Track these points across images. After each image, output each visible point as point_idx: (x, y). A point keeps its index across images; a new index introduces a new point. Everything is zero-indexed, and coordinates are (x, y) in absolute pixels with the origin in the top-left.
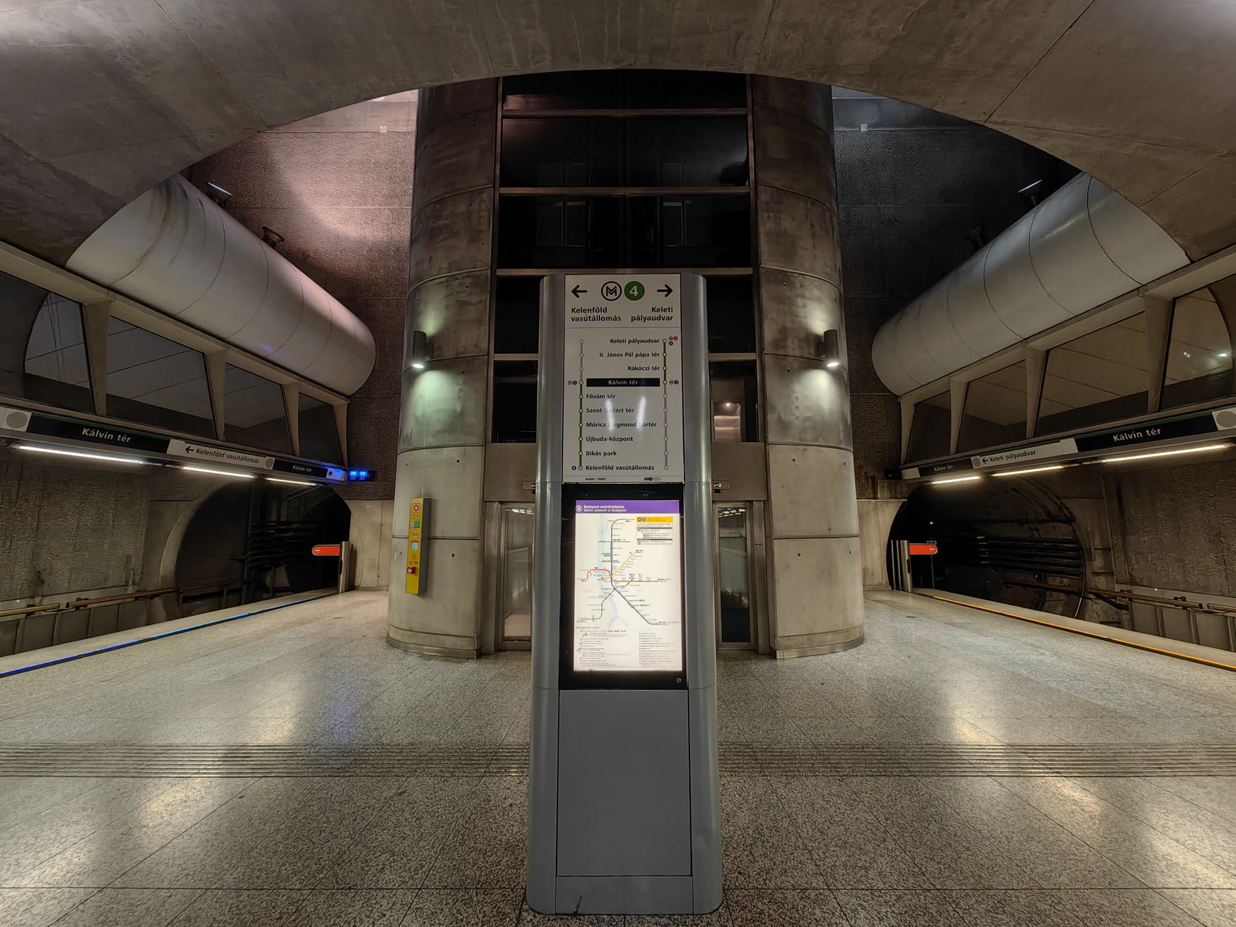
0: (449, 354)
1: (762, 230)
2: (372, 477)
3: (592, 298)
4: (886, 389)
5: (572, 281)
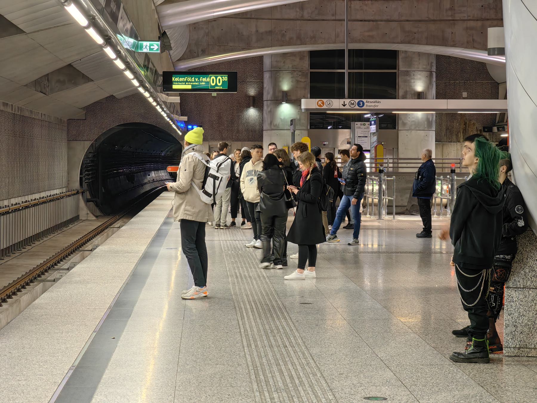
0: (293, 98)
1: (400, 57)
3: (359, 125)
4: (492, 79)
5: (356, 123)
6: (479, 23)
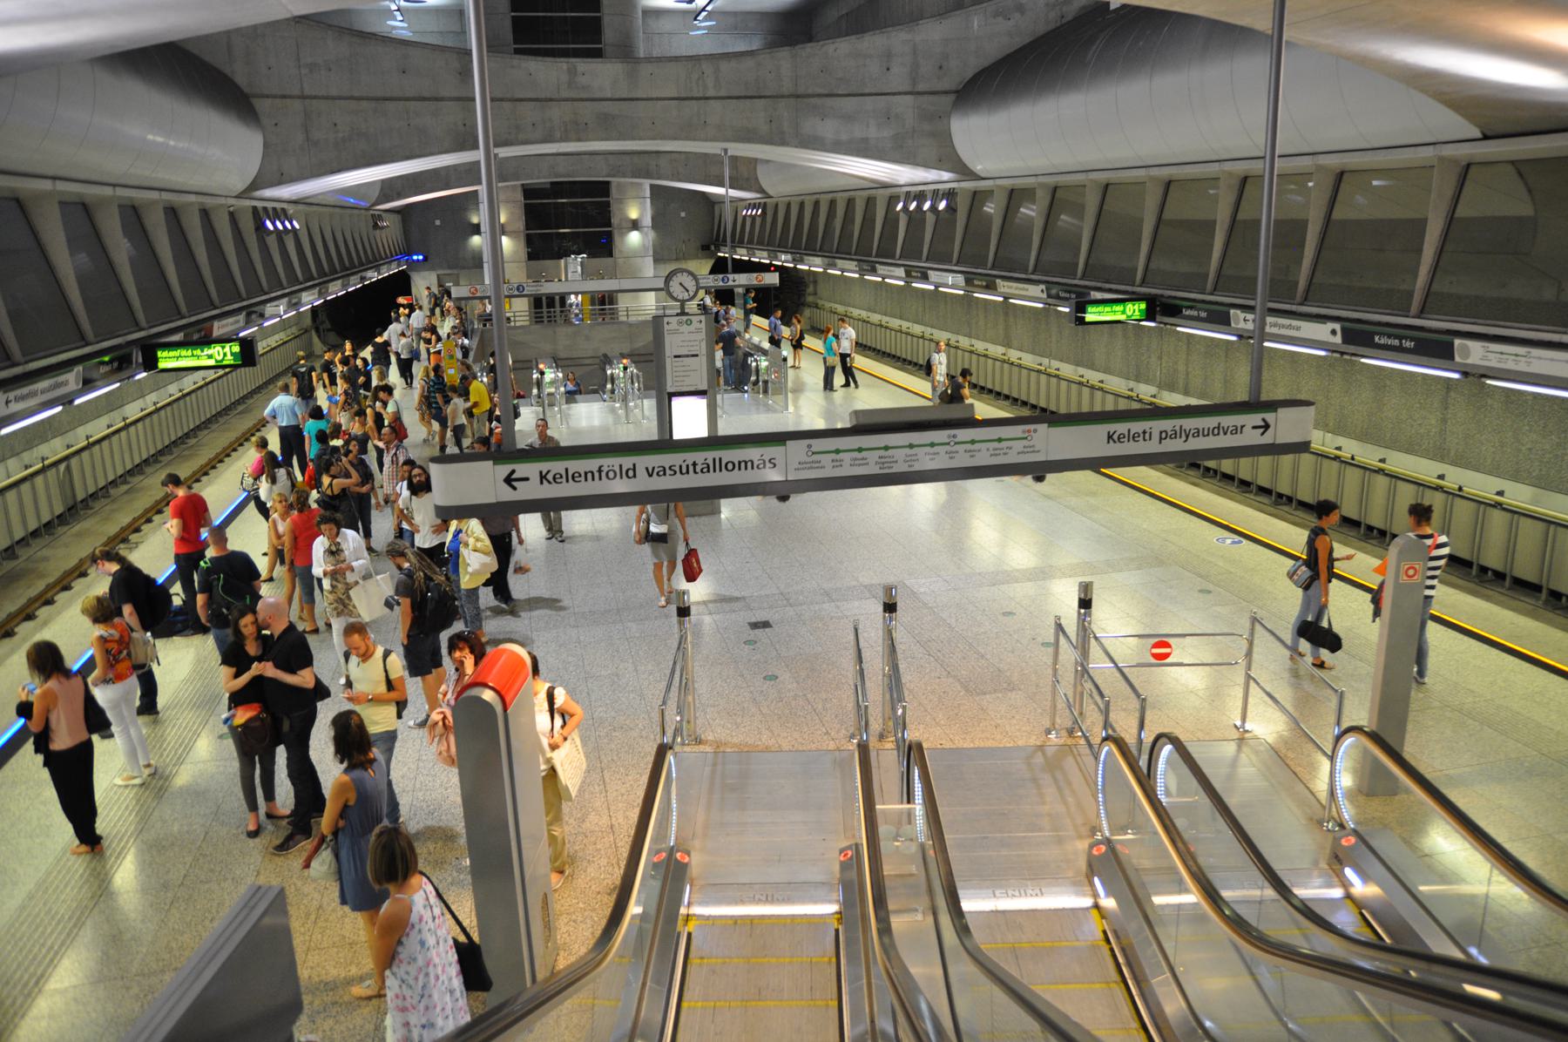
2: (425, 259)
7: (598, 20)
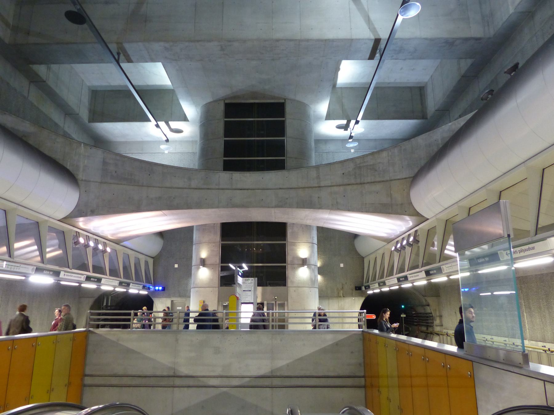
2: (164, 289)
4: (359, 255)
6: (342, 188)
7: (283, 123)
